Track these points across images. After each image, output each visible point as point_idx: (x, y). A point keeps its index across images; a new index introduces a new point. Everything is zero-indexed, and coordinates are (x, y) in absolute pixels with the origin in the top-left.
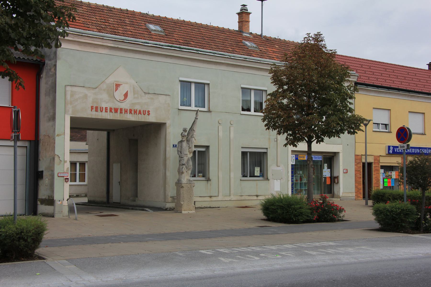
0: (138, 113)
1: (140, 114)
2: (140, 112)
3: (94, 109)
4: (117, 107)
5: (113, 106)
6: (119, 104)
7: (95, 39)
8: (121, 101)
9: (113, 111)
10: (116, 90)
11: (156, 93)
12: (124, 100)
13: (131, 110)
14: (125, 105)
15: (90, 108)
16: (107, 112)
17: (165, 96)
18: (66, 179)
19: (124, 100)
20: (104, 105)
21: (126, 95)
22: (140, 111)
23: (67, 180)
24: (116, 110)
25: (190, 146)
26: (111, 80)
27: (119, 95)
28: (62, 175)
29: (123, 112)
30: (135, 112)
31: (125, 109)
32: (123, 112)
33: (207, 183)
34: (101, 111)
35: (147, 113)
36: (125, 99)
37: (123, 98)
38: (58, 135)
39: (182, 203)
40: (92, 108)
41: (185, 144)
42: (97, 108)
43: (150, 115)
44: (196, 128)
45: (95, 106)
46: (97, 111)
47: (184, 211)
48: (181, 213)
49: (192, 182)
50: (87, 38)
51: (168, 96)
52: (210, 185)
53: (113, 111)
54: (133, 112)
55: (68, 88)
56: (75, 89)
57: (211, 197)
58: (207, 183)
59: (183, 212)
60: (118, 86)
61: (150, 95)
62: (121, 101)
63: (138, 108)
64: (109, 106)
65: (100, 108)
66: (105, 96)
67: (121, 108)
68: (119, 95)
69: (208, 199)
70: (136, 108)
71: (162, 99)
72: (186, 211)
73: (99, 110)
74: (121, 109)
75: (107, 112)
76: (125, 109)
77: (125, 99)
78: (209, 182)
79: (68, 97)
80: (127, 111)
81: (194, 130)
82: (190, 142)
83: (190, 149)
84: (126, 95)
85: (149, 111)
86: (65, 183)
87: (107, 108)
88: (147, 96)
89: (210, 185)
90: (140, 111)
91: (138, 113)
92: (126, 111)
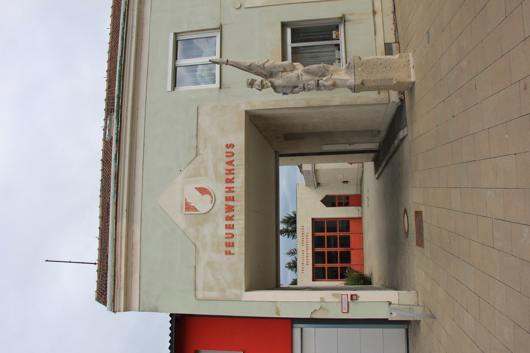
0: (231, 167)
1: (233, 163)
2: (230, 163)
3: (230, 249)
4: (224, 207)
5: (222, 214)
6: (218, 202)
7: (118, 252)
8: (214, 200)
9: (230, 214)
10: (196, 210)
11: (195, 133)
12: (211, 195)
13: (229, 181)
14: (220, 194)
15: (229, 256)
16: (233, 225)
17: (200, 116)
18: (352, 299)
19: (211, 195)
20: (223, 231)
21: (203, 191)
22: (228, 163)
23: (354, 297)
24: (230, 209)
25: (282, 69)
26: (180, 218)
27: (203, 204)
28: (345, 306)
29: (230, 195)
30: (230, 172)
31: (226, 192)
32: (230, 195)
33: (349, 21)
34: (233, 236)
35: (230, 150)
36: (210, 193)
37: (207, 197)
38: (278, 313)
39: (395, 82)
40: (228, 253)
41: (278, 81)
42: (228, 245)
43: (233, 143)
44: (247, 61)
45: (224, 248)
46: (233, 243)
47: (410, 77)
48: (414, 83)
49: (352, 62)
50: (118, 266)
51: (200, 111)
52: (352, 14)
53: (230, 214)
54: (230, 177)
55: (200, 295)
56: (200, 284)
57: (374, 13)
58: (349, 21)
59: (413, 79)
60: (189, 207)
61: (201, 145)
62: (214, 200)
63: (222, 167)
64: (223, 223)
65: (227, 238)
66: (207, 230)
67: (224, 199)
68: (203, 204)
69: (379, 17)
70: (224, 172)
71: (205, 122)
72: (410, 71)
73: (230, 240)
74: (228, 199)
75: (233, 225)
76: (226, 192)
77: (210, 193)
78: (347, 17)
79: (213, 294)
80: (230, 188)
81: (251, 65)
82: (273, 70)
83: (287, 70)
84: (203, 191)
85: (228, 146)
86: (360, 299)
87: (226, 225)
88: (201, 151)
89: (352, 14)
90: (228, 163)
91: (231, 167)
92: (230, 190)
